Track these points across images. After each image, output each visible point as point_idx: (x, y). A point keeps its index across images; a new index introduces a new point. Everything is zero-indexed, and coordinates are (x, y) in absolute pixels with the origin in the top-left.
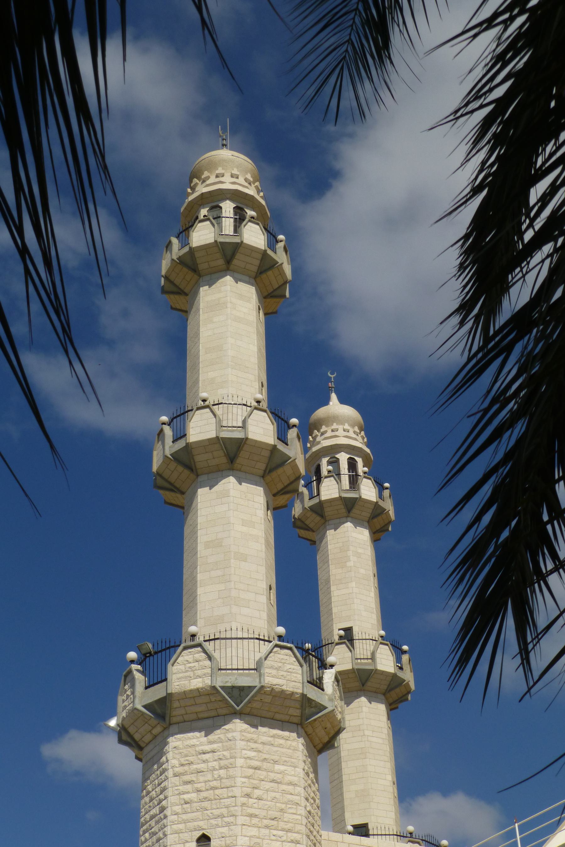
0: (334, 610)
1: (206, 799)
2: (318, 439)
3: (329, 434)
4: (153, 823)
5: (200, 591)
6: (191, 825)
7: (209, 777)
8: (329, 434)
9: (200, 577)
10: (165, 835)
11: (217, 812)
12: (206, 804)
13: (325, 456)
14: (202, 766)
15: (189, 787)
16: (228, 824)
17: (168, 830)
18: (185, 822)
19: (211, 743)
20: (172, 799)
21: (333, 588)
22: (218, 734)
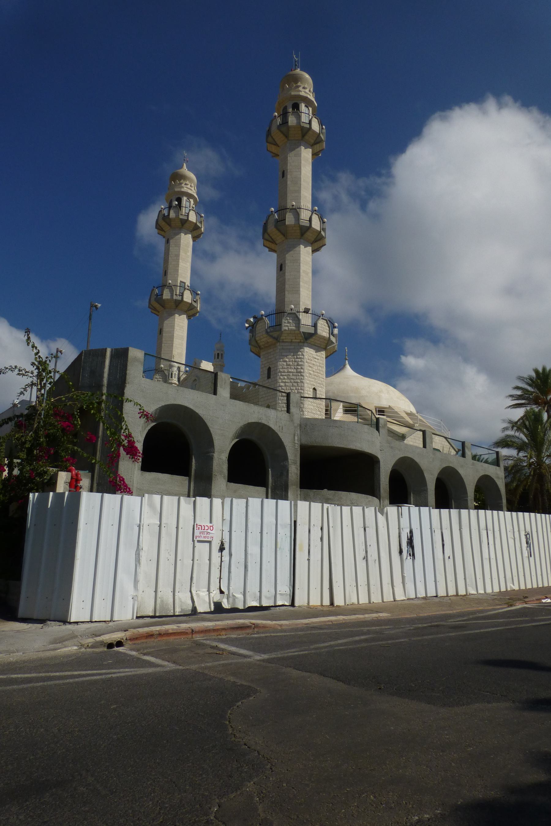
0: (180, 271)
1: (315, 375)
2: (183, 185)
3: (189, 186)
4: (291, 374)
5: (301, 289)
6: (312, 383)
7: (316, 368)
8: (189, 186)
9: (301, 283)
10: (302, 382)
11: (319, 382)
12: (316, 377)
13: (186, 196)
14: (315, 363)
15: (310, 369)
16: (322, 387)
17: (304, 381)
18: (310, 381)
19: (317, 355)
20: (306, 371)
21: (180, 261)
22: (319, 354)
